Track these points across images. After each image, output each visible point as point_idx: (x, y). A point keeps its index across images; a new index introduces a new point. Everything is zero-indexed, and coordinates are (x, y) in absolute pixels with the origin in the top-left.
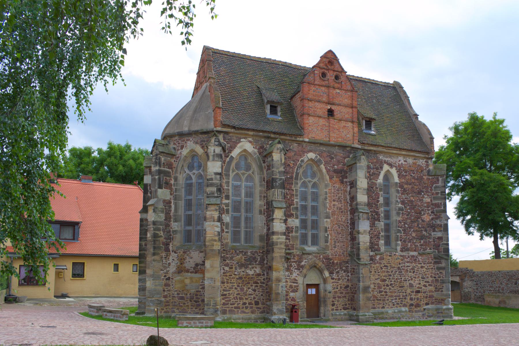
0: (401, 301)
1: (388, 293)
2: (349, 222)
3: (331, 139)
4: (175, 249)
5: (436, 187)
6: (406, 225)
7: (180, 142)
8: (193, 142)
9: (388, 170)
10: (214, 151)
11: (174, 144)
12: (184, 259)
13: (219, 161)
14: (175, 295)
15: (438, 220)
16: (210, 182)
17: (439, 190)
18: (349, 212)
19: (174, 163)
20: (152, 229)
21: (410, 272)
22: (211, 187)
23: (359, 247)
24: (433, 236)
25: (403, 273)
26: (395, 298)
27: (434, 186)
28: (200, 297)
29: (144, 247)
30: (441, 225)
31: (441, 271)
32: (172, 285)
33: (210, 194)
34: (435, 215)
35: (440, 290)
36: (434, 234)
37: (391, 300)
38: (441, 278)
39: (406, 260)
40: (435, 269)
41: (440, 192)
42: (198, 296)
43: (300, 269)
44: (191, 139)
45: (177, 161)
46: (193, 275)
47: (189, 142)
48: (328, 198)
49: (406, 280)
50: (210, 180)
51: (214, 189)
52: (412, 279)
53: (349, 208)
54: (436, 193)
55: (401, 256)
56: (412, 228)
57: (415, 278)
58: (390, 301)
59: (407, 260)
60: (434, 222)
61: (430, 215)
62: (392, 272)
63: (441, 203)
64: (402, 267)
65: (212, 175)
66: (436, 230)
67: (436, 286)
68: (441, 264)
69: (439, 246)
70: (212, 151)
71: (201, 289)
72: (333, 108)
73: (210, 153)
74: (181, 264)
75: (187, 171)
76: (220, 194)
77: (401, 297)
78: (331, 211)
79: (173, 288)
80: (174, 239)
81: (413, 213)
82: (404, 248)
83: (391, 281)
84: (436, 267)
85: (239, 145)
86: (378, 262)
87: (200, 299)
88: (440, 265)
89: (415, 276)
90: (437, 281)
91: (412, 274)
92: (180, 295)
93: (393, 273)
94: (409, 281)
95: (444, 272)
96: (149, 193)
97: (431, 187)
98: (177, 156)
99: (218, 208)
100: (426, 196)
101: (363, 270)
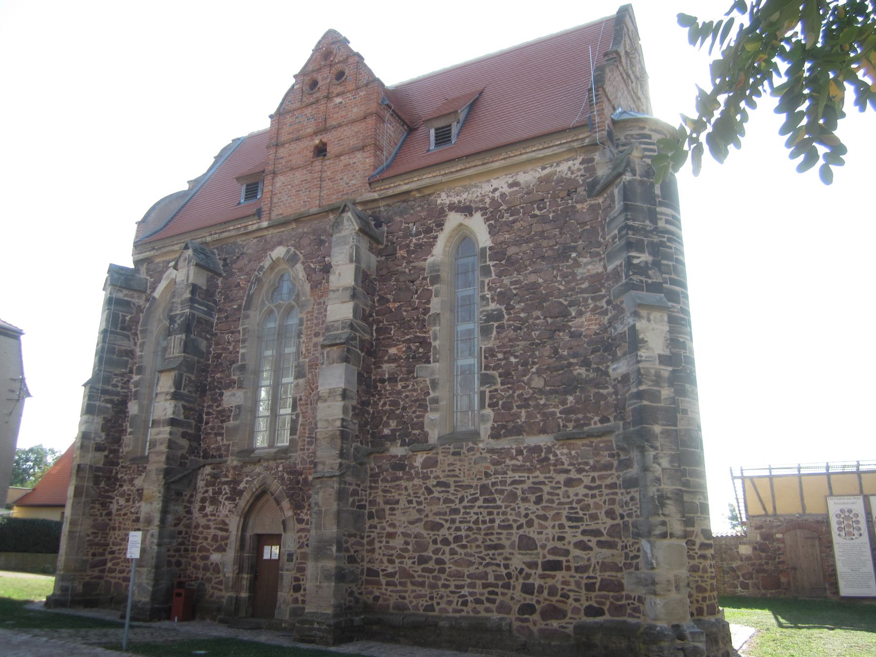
0: (490, 593)
1: (446, 566)
6: (513, 359)
9: (461, 225)
21: (524, 500)
25: (499, 503)
26: (469, 581)
37: (457, 587)
39: (508, 462)
43: (234, 500)
48: (304, 331)
49: (510, 527)
52: (530, 524)
55: (492, 451)
56: (534, 363)
57: (545, 518)
58: (452, 588)
59: (514, 462)
61: (605, 313)
62: (462, 500)
64: (494, 484)
72: (325, 140)
77: (491, 579)
78: (307, 360)
81: (538, 318)
82: (504, 427)
83: (458, 529)
85: (165, 275)
86: (417, 473)
89: (541, 512)
91: (533, 507)
93: (465, 503)
94: (520, 527)
100: (583, 260)
101: (321, 494)
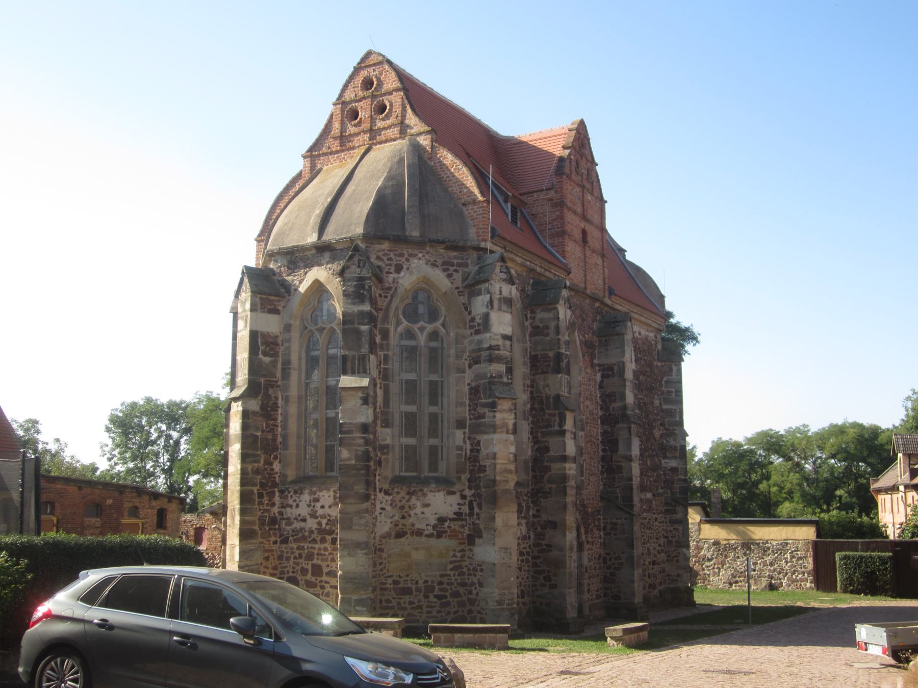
2: (600, 438)
3: (589, 286)
4: (386, 486)
5: (667, 382)
7: (392, 256)
8: (424, 261)
10: (501, 291)
11: (378, 258)
12: (410, 507)
13: (508, 312)
14: (388, 586)
15: (672, 439)
16: (496, 352)
17: (673, 388)
18: (599, 420)
19: (379, 299)
20: (361, 441)
22: (497, 362)
23: (632, 484)
24: (663, 465)
27: (665, 379)
28: (449, 587)
29: (250, 475)
30: (676, 447)
31: (676, 526)
32: (381, 564)
33: (495, 377)
34: (667, 429)
35: (675, 559)
36: (665, 462)
38: (677, 538)
40: (666, 522)
41: (674, 390)
42: (445, 586)
44: (420, 255)
45: (386, 297)
46: (433, 541)
47: (416, 261)
50: (495, 350)
51: (502, 368)
53: (600, 413)
54: (668, 392)
60: (665, 441)
63: (675, 410)
65: (498, 340)
66: (668, 455)
67: (669, 552)
68: (676, 513)
69: (673, 483)
70: (498, 292)
71: (451, 570)
73: (495, 294)
74: (403, 517)
75: (405, 323)
76: (511, 379)
79: (381, 570)
80: (383, 465)
84: (668, 520)
87: (450, 591)
88: (675, 517)
90: (670, 542)
92: (401, 585)
95: (681, 528)
96: (260, 352)
97: (660, 381)
98: (387, 285)
99: (512, 408)
